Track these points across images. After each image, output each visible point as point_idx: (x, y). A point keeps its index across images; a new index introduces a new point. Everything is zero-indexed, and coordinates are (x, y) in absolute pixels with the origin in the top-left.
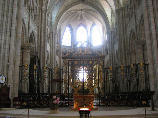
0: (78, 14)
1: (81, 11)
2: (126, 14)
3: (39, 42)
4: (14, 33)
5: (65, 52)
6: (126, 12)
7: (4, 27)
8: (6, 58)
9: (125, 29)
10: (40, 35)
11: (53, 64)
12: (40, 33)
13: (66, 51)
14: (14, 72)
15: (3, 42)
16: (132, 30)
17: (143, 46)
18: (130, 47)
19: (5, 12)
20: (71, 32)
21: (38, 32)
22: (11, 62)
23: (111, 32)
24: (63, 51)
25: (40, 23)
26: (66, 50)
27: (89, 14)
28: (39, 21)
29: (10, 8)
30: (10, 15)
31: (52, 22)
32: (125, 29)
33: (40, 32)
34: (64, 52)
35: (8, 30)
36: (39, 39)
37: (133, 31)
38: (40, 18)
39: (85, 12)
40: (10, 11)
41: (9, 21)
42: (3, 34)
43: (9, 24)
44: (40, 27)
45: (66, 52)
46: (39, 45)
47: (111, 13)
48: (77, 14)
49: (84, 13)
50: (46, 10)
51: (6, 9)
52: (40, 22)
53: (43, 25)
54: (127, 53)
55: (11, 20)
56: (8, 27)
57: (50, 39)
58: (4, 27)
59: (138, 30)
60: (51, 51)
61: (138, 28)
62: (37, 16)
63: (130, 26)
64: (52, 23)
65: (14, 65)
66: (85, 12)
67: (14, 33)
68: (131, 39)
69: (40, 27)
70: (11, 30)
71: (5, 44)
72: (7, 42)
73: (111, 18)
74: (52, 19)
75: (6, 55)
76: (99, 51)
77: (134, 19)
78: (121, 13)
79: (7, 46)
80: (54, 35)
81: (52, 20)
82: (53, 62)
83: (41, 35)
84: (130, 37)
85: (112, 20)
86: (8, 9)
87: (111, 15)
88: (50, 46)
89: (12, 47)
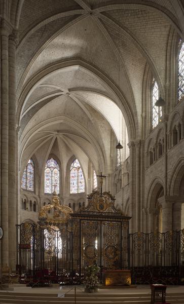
0: (52, 137)
1: (57, 133)
2: (145, 152)
6: (146, 149)
9: (142, 175)
16: (156, 178)
17: (173, 204)
18: (147, 204)
20: (34, 167)
23: (109, 175)
26: (27, 198)
27: (69, 140)
32: (142, 175)
34: (23, 200)
37: (157, 180)
39: (64, 135)
47: (110, 144)
48: (49, 137)
49: (61, 136)
54: (142, 212)
59: (168, 180)
61: (169, 177)
63: (152, 172)
66: (64, 135)
68: (151, 191)
73: (110, 152)
76: (80, 203)
77: (164, 163)
78: (137, 149)
84: (150, 188)
85: (111, 156)
87: (110, 146)
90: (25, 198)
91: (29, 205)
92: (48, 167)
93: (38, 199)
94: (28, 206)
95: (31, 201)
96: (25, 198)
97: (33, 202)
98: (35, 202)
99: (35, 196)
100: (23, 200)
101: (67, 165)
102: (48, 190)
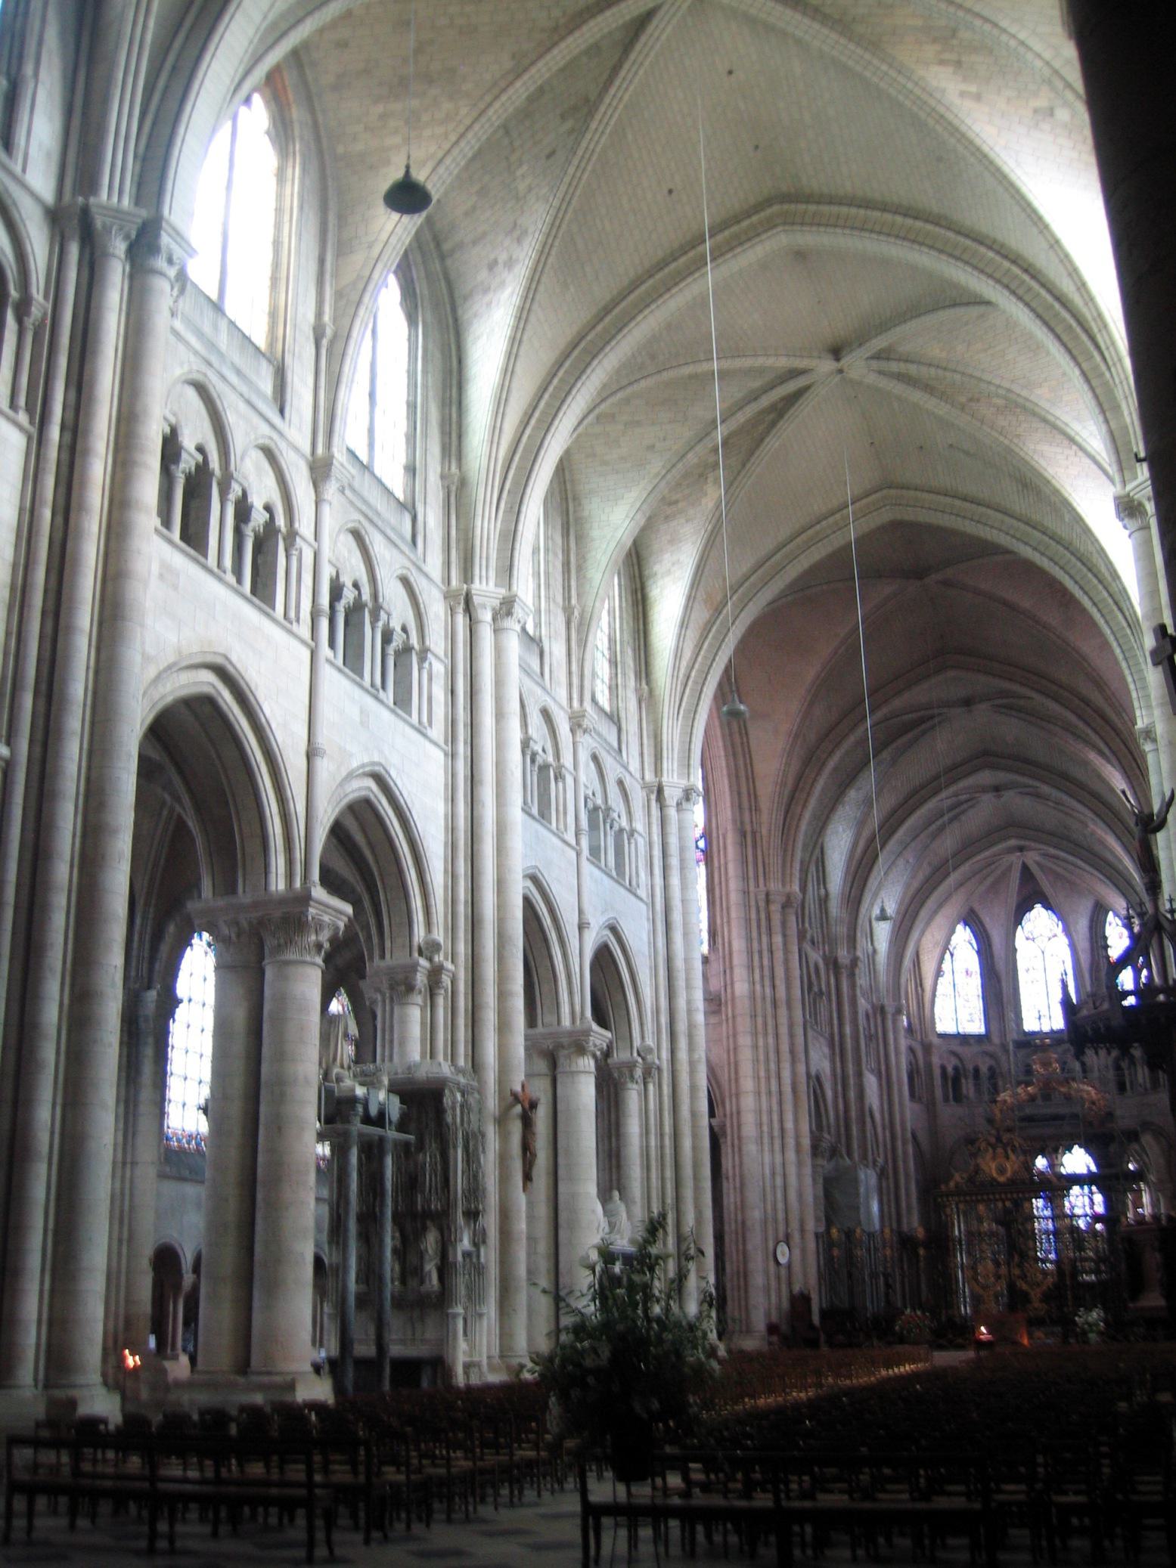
3: (840, 1101)
4: (791, 1142)
5: (956, 1069)
7: (765, 1128)
8: (781, 1216)
10: (839, 1070)
11: (901, 1163)
12: (838, 1064)
13: (960, 1065)
14: (803, 1250)
15: (767, 1172)
19: (763, 1081)
20: (978, 952)
21: (833, 1062)
22: (795, 1225)
24: (943, 1068)
25: (835, 1022)
28: (831, 1012)
29: (773, 1066)
30: (774, 1088)
31: (875, 951)
33: (838, 1059)
34: (950, 1070)
35: (776, 1133)
36: (840, 1088)
38: (834, 998)
40: (773, 1074)
41: (775, 1107)
42: (766, 1148)
43: (775, 1117)
44: (837, 1038)
45: (962, 1072)
46: (841, 1113)
49: (1037, 858)
50: (855, 961)
51: (762, 1074)
52: (835, 1015)
53: (848, 1030)
55: (780, 1103)
56: (776, 1125)
57: (874, 1041)
58: (765, 1128)
60: (885, 1097)
62: (821, 993)
64: (874, 961)
65: (802, 1231)
67: (791, 1142)
69: (837, 1038)
70: (782, 1130)
71: (773, 1174)
72: (779, 1169)
74: (875, 938)
75: (780, 1206)
79: (779, 1181)
80: (889, 1017)
81: (876, 944)
82: (900, 1151)
83: (843, 1071)
86: (768, 1070)
88: (880, 1078)
89: (793, 1180)
90: (954, 1061)
91: (971, 1081)
92: (1027, 939)
93: (1003, 1058)
94: (968, 1087)
95: (977, 1070)
96: (954, 1061)
97: (984, 1069)
98: (991, 1069)
99: (990, 1049)
100: (950, 1070)
101: (1092, 921)
102: (1030, 1024)
